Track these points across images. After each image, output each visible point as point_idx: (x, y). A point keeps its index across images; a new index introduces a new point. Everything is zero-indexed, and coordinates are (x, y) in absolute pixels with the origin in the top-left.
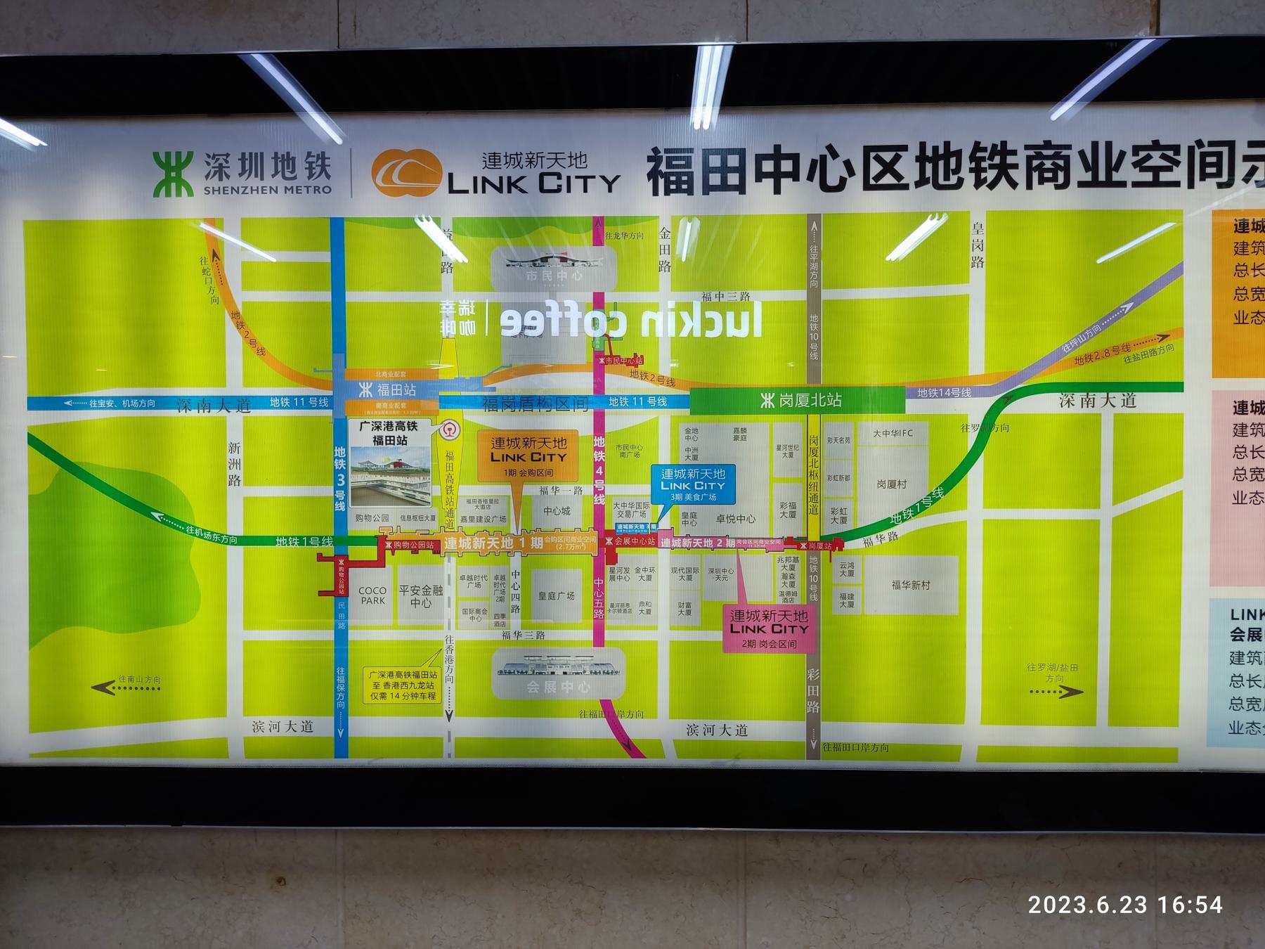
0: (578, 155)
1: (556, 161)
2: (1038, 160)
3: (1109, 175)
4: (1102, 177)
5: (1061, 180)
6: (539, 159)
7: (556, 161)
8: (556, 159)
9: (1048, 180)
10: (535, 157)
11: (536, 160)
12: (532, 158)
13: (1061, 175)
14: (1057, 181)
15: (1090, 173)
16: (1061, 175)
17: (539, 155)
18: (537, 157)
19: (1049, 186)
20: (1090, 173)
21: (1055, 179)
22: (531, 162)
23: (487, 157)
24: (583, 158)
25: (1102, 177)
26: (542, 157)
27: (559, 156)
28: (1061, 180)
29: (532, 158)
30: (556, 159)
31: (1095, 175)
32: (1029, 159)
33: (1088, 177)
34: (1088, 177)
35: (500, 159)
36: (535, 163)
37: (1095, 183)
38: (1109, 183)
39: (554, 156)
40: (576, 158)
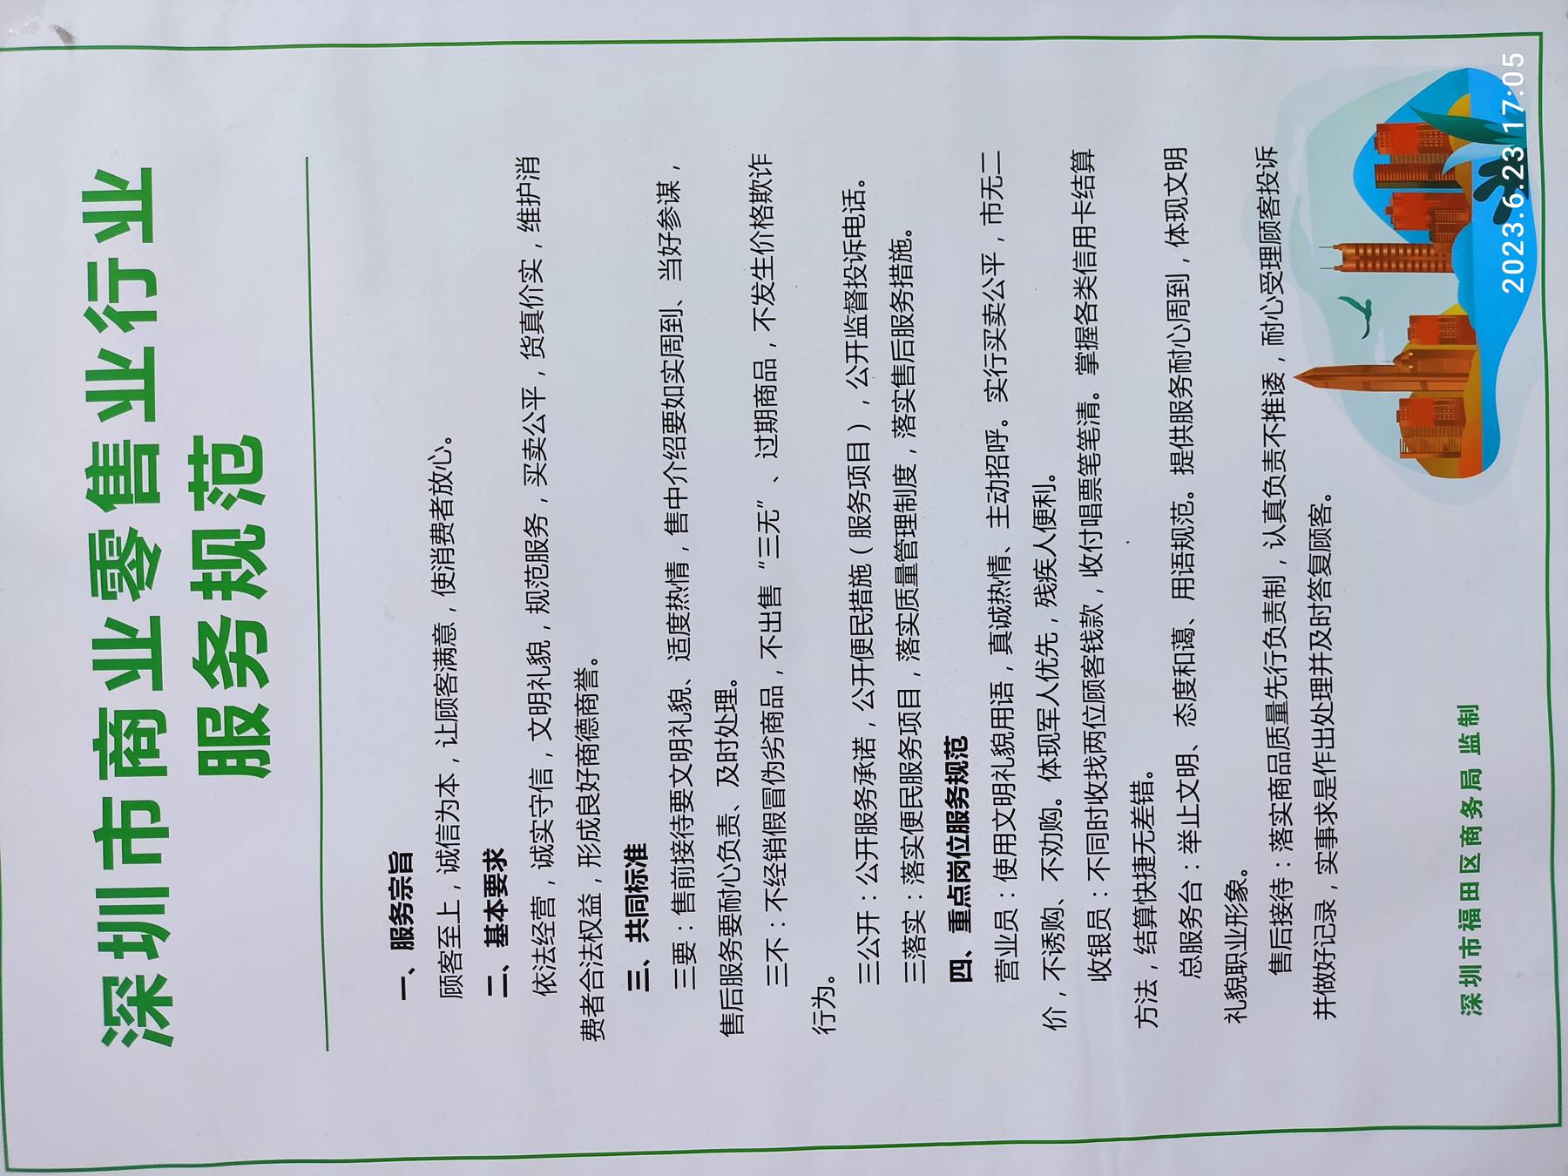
2: (121, 757)
5: (152, 724)
9: (151, 742)
13: (144, 724)
14: (154, 729)
16: (144, 724)
21: (149, 733)
28: (152, 724)
32: (120, 772)
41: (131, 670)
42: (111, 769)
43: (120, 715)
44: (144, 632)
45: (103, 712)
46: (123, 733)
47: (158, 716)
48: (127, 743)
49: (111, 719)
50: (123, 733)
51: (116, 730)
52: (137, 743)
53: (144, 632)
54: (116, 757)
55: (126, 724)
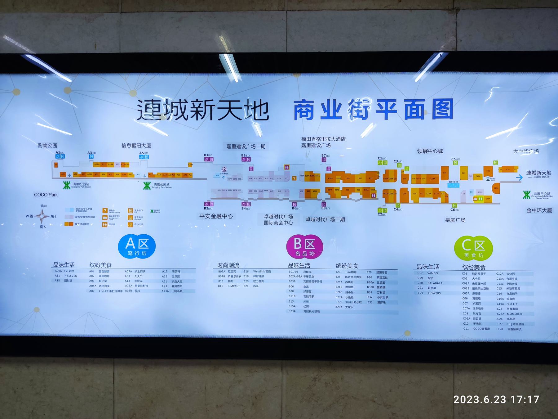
0: (258, 104)
1: (230, 111)
3: (334, 114)
4: (331, 115)
5: (309, 116)
6: (208, 108)
7: (230, 111)
8: (230, 108)
9: (304, 116)
10: (203, 105)
11: (203, 109)
12: (199, 107)
15: (326, 113)
16: (309, 114)
17: (208, 103)
18: (206, 106)
19: (304, 119)
20: (326, 113)
21: (307, 115)
22: (197, 112)
23: (143, 105)
24: (264, 108)
25: (331, 115)
26: (211, 106)
27: (233, 105)
28: (309, 116)
29: (199, 107)
30: (230, 108)
31: (328, 114)
33: (325, 115)
34: (325, 115)
35: (159, 108)
36: (202, 114)
37: (328, 117)
38: (334, 117)
39: (226, 105)
40: (255, 108)
41: (326, 110)
42: (297, 104)
43: (312, 107)
44: (337, 115)
45: (313, 102)
46: (307, 108)
47: (311, 118)
48: (304, 109)
49: (311, 104)
50: (307, 108)
51: (308, 106)
52: (304, 112)
53: (337, 115)
54: (300, 106)
55: (310, 109)
